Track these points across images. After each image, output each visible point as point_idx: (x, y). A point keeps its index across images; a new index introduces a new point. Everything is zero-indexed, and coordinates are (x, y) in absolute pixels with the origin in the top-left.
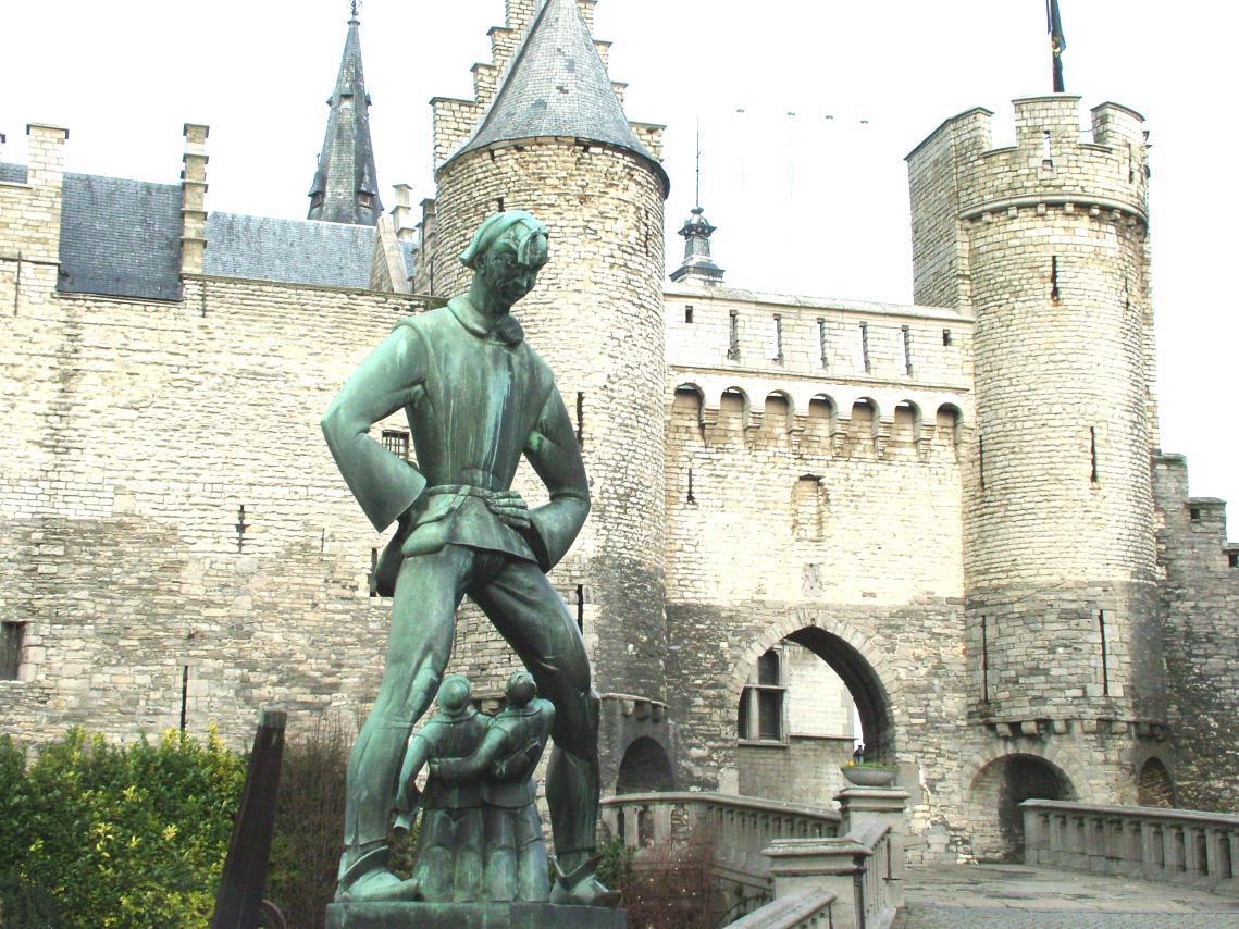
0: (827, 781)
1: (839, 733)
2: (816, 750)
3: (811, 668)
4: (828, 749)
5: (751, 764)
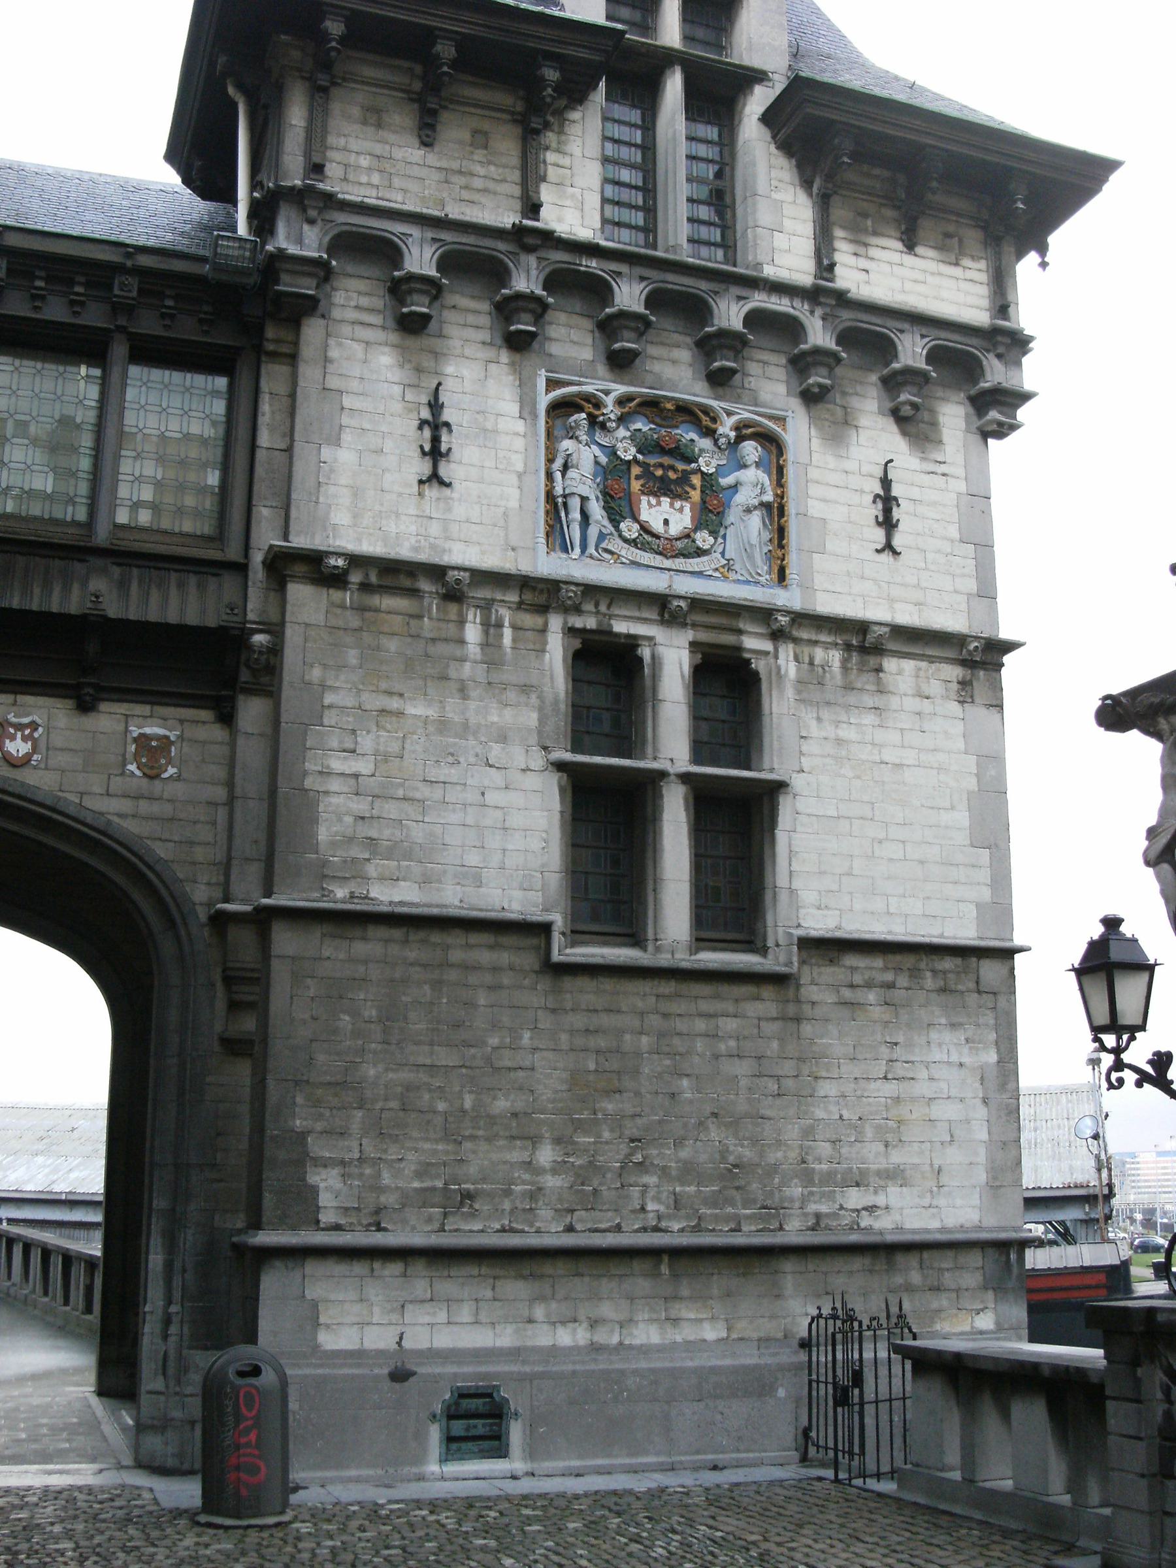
0: (923, 1088)
1: (964, 932)
2: (891, 986)
3: (869, 719)
4: (929, 982)
5: (661, 1035)
